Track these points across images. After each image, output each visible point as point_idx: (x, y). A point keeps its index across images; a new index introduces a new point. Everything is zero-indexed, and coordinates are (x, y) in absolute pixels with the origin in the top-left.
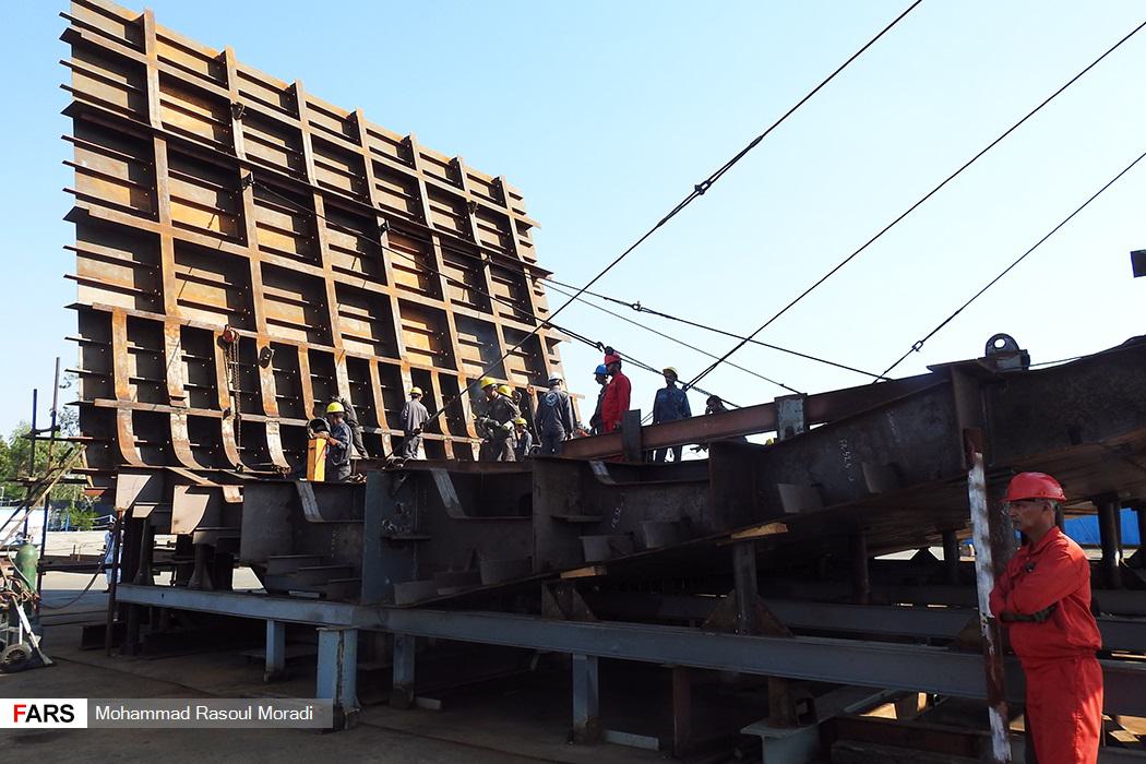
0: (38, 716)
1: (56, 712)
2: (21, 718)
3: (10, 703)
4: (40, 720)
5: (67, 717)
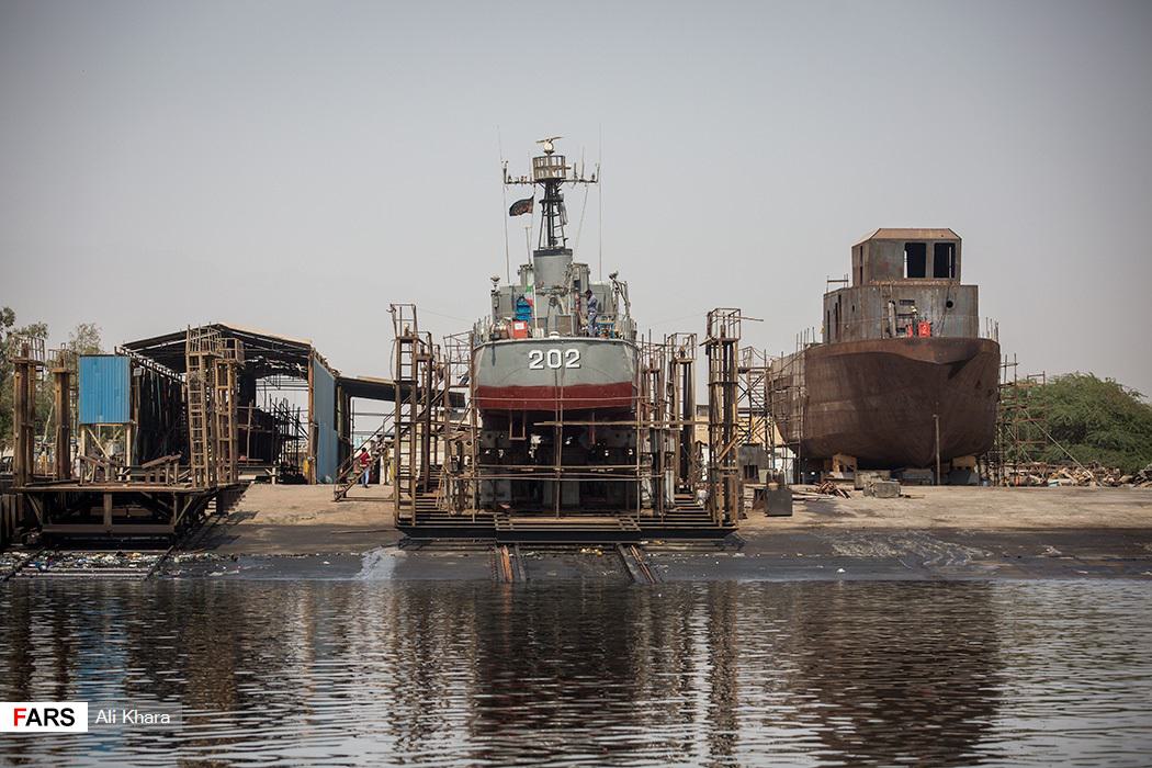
0: (38, 720)
1: (56, 715)
2: (21, 722)
3: (8, 708)
4: (40, 724)
5: (68, 721)
